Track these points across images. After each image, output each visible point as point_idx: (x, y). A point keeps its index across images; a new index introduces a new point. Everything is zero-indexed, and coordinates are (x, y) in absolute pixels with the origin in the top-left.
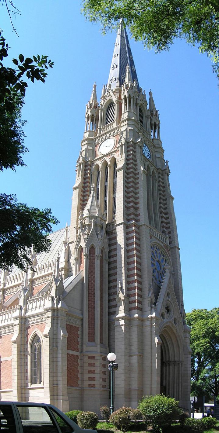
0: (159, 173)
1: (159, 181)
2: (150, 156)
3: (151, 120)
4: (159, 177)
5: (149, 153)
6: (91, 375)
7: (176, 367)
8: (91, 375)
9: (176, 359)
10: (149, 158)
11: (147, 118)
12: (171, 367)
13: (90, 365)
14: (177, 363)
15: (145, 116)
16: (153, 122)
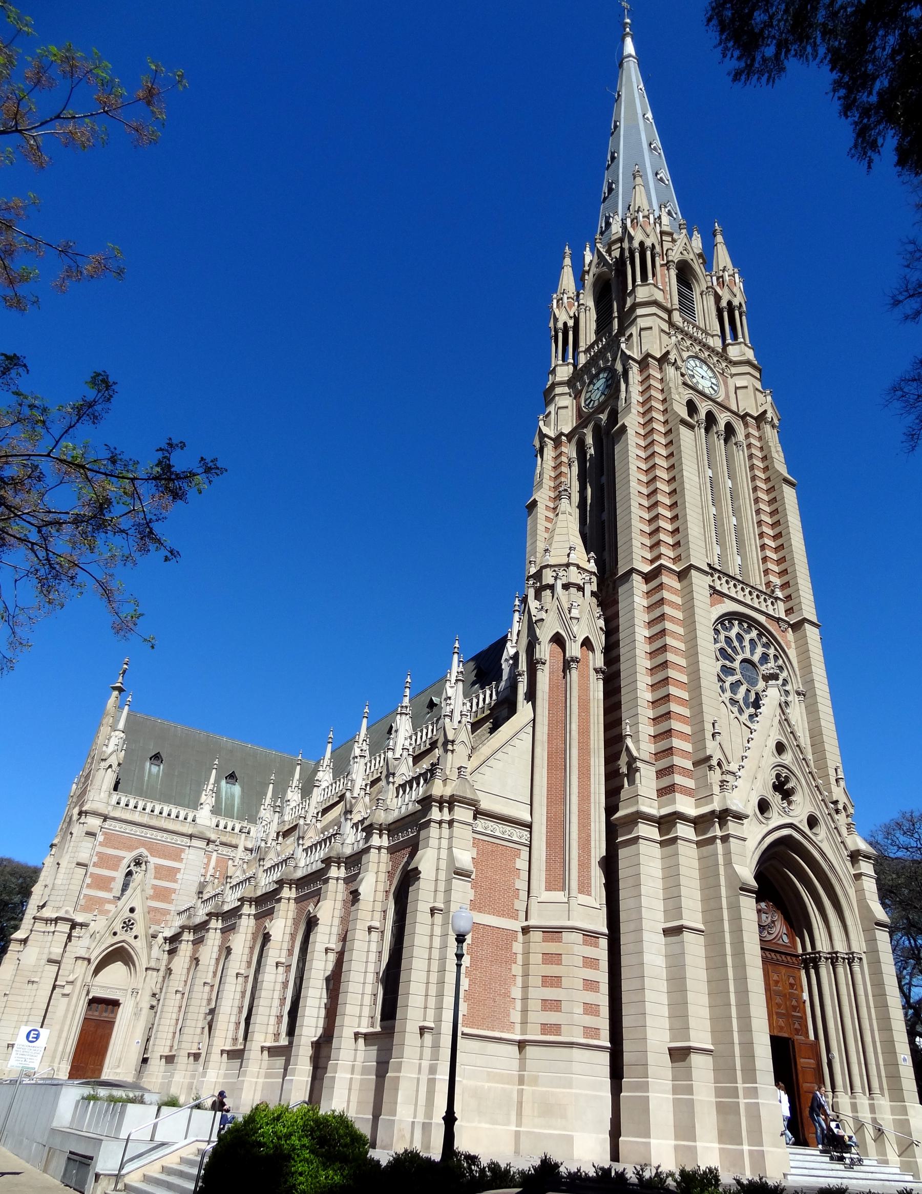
0: (746, 425)
1: (749, 446)
2: (715, 388)
3: (718, 298)
4: (748, 436)
5: (714, 381)
6: (551, 993)
7: (840, 970)
8: (551, 993)
9: (840, 947)
10: (713, 392)
11: (704, 296)
12: (823, 971)
13: (551, 958)
14: (844, 959)
15: (698, 292)
16: (724, 303)
